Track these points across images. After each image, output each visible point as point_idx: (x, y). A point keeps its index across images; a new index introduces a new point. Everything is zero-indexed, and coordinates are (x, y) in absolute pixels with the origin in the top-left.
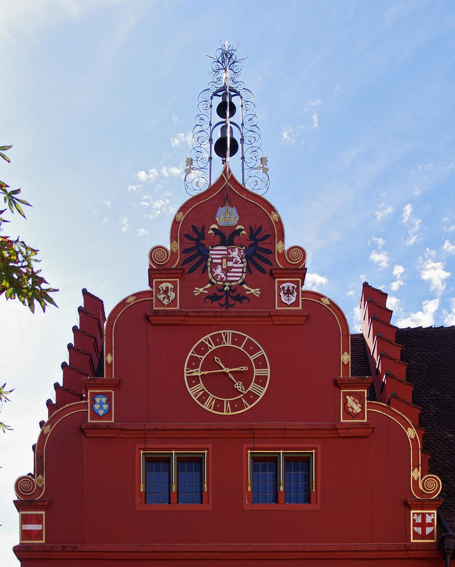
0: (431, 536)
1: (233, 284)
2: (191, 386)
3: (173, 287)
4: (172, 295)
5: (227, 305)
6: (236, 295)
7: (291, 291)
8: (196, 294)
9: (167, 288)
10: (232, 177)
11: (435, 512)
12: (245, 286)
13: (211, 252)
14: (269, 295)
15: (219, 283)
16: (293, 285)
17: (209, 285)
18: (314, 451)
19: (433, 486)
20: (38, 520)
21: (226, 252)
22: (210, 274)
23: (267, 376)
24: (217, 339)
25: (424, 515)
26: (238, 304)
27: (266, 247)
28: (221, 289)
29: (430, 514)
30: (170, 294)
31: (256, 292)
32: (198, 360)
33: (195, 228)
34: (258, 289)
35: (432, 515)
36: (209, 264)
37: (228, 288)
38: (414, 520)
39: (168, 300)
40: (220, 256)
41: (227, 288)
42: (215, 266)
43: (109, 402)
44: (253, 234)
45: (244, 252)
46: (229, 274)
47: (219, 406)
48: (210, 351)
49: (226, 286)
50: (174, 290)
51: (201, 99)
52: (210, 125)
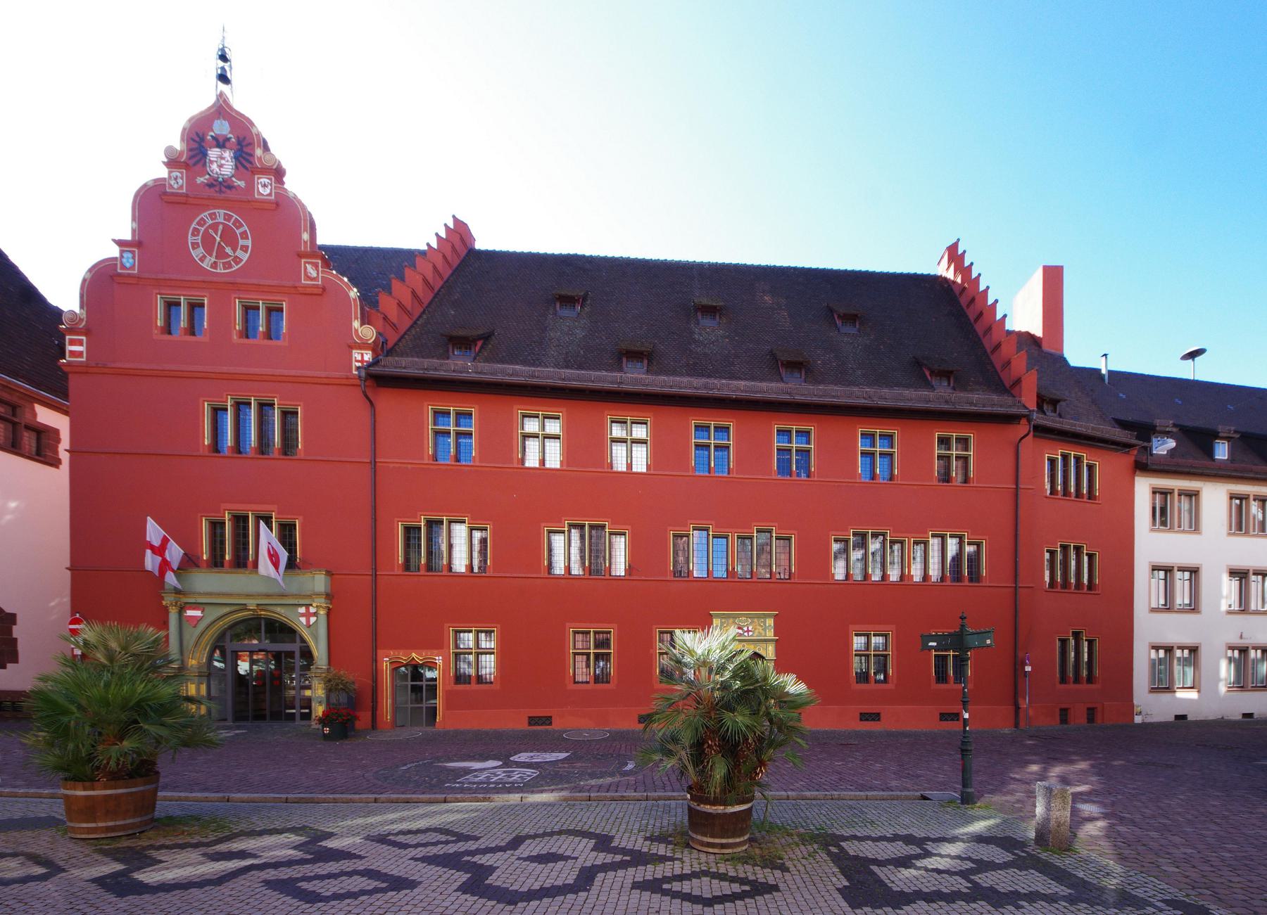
4: (180, 181)
5: (221, 191)
6: (226, 185)
14: (251, 187)
24: (213, 216)
28: (216, 180)
31: (242, 184)
42: (211, 162)
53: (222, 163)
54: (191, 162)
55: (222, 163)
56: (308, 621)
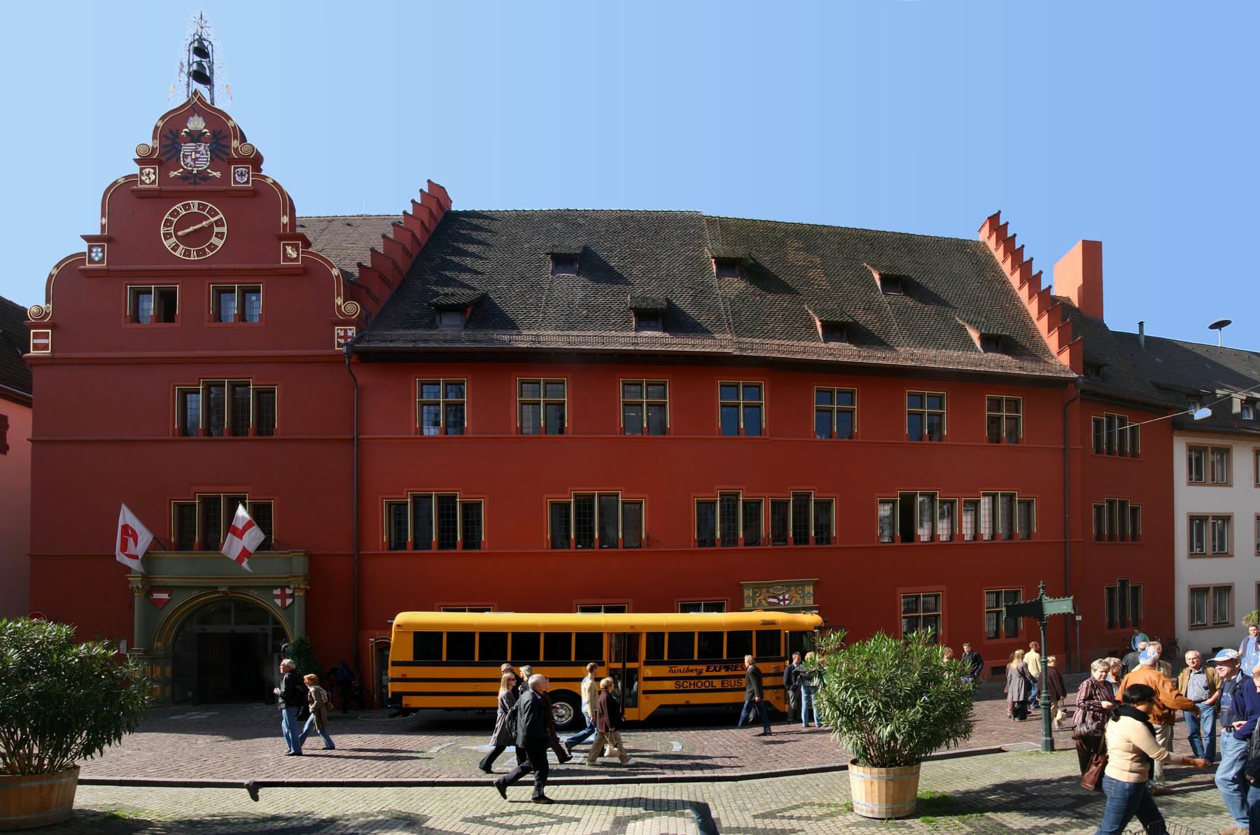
4: (153, 177)
5: (195, 183)
6: (203, 176)
20: (46, 336)
25: (346, 331)
30: (150, 177)
31: (218, 174)
33: (171, 131)
42: (185, 156)
43: (103, 251)
44: (215, 134)
47: (187, 253)
53: (196, 157)
54: (164, 158)
55: (196, 157)
56: (283, 602)
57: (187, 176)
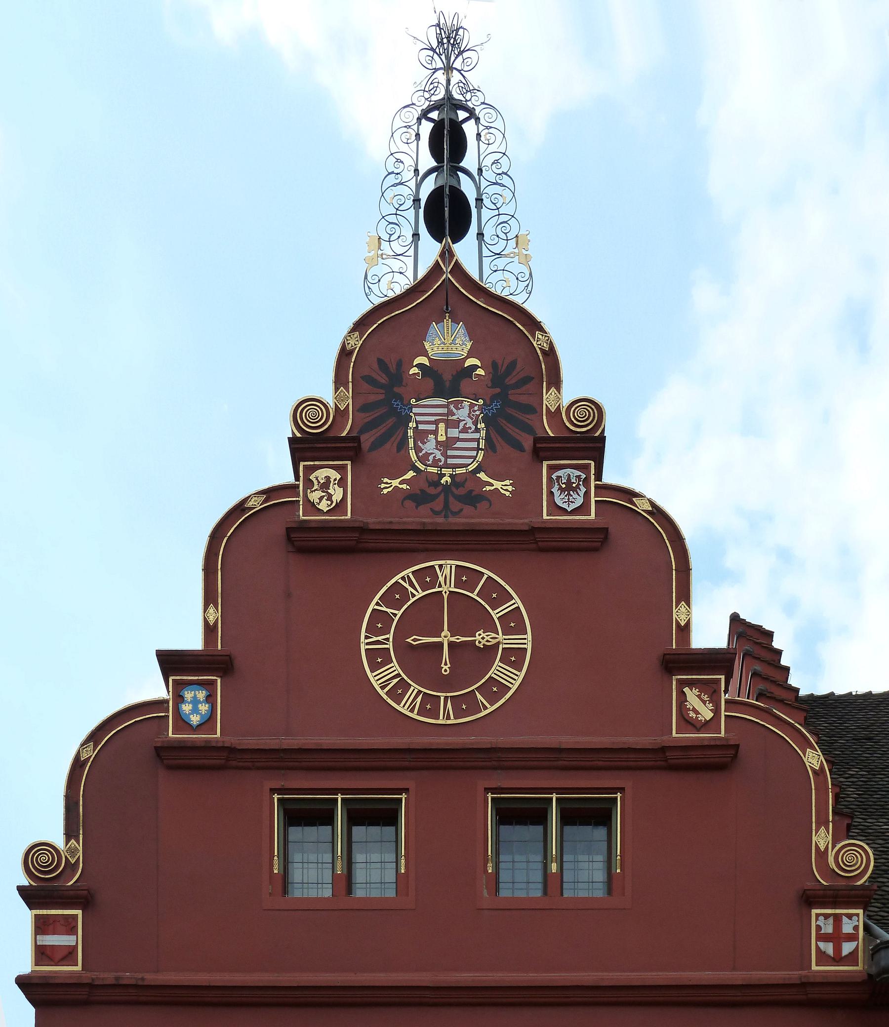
0: (852, 958)
1: (459, 471)
2: (374, 667)
3: (338, 477)
6: (466, 491)
7: (574, 485)
8: (385, 491)
9: (328, 478)
10: (457, 265)
11: (860, 912)
12: (482, 476)
13: (415, 410)
14: (528, 491)
15: (430, 469)
16: (578, 473)
17: (411, 474)
18: (619, 795)
19: (857, 862)
21: (445, 411)
22: (412, 454)
23: (526, 649)
25: (837, 919)
26: (468, 509)
27: (524, 399)
29: (850, 916)
31: (504, 487)
32: (388, 618)
34: (507, 482)
35: (855, 918)
36: (410, 433)
37: (449, 480)
38: (819, 928)
39: (329, 503)
40: (433, 418)
41: (446, 479)
42: (421, 436)
44: (499, 376)
45: (481, 408)
46: (450, 453)
48: (412, 600)
49: (444, 475)
50: (342, 483)
51: (398, 123)
52: (416, 171)
53: (448, 438)
55: (448, 438)
57: (426, 491)
